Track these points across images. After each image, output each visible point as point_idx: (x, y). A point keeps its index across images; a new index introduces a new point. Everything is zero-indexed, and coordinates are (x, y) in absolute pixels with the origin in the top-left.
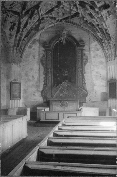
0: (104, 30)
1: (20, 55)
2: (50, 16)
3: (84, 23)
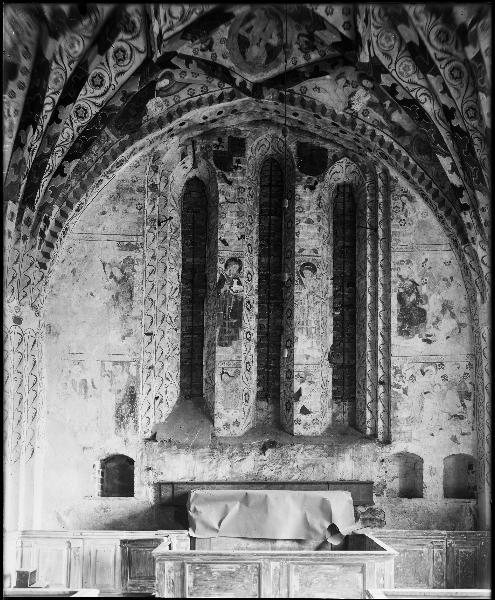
0: (476, 141)
1: (36, 253)
2: (200, 55)
3: (370, 109)
